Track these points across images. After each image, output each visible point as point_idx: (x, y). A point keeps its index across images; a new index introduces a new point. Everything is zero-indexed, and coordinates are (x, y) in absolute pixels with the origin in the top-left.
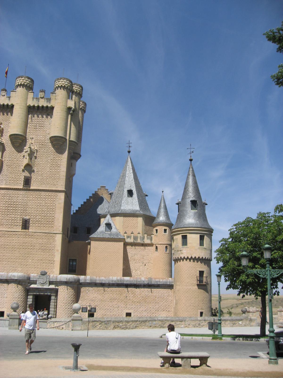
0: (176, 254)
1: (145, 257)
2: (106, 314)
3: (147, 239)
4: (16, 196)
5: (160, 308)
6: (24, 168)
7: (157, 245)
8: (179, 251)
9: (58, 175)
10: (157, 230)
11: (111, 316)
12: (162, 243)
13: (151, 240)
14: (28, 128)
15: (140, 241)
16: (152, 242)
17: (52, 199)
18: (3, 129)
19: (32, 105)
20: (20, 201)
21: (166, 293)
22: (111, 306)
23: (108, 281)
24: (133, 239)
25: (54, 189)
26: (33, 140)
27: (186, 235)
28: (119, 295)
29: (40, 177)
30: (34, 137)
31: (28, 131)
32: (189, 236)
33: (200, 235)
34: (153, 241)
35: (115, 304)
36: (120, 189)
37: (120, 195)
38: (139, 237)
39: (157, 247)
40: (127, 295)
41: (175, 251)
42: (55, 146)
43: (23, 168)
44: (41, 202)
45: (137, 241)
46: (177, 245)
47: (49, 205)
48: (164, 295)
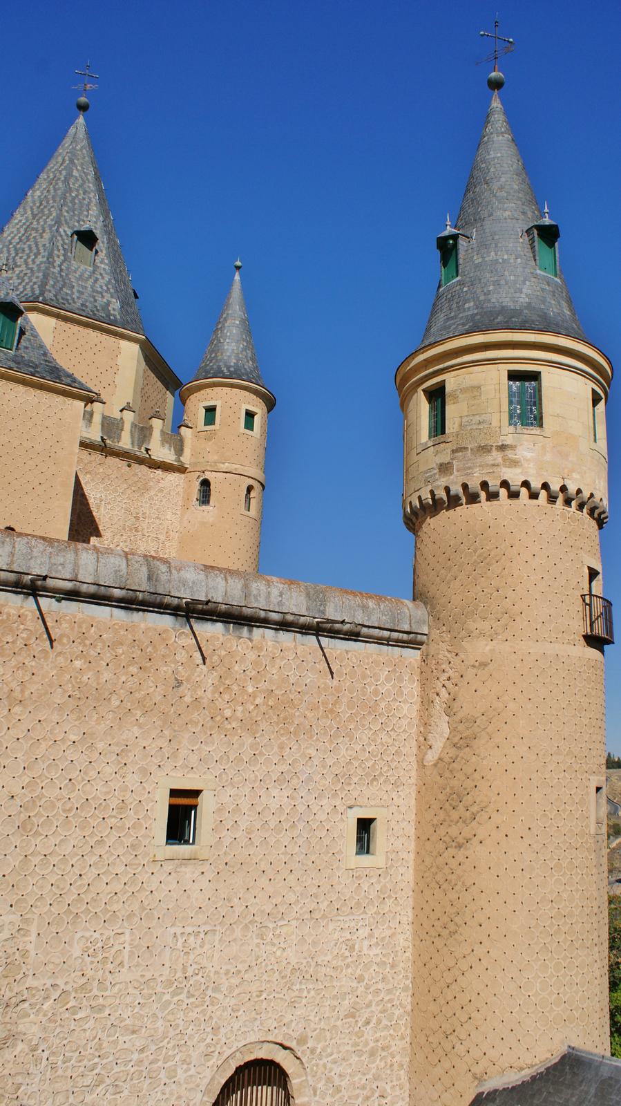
0: (469, 468)
1: (145, 525)
2: (39, 797)
3: (163, 445)
5: (356, 764)
7: (208, 475)
8: (489, 451)
10: (211, 411)
11: (70, 810)
12: (236, 469)
13: (179, 451)
15: (133, 443)
16: (182, 459)
21: (388, 679)
22: (73, 738)
23: (69, 567)
24: (100, 427)
27: (535, 376)
28: (133, 669)
32: (552, 380)
34: (186, 458)
35: (103, 727)
36: (38, 223)
37: (37, 245)
38: (127, 427)
39: (206, 483)
40: (183, 673)
41: (453, 451)
45: (118, 442)
46: (477, 418)
48: (376, 692)
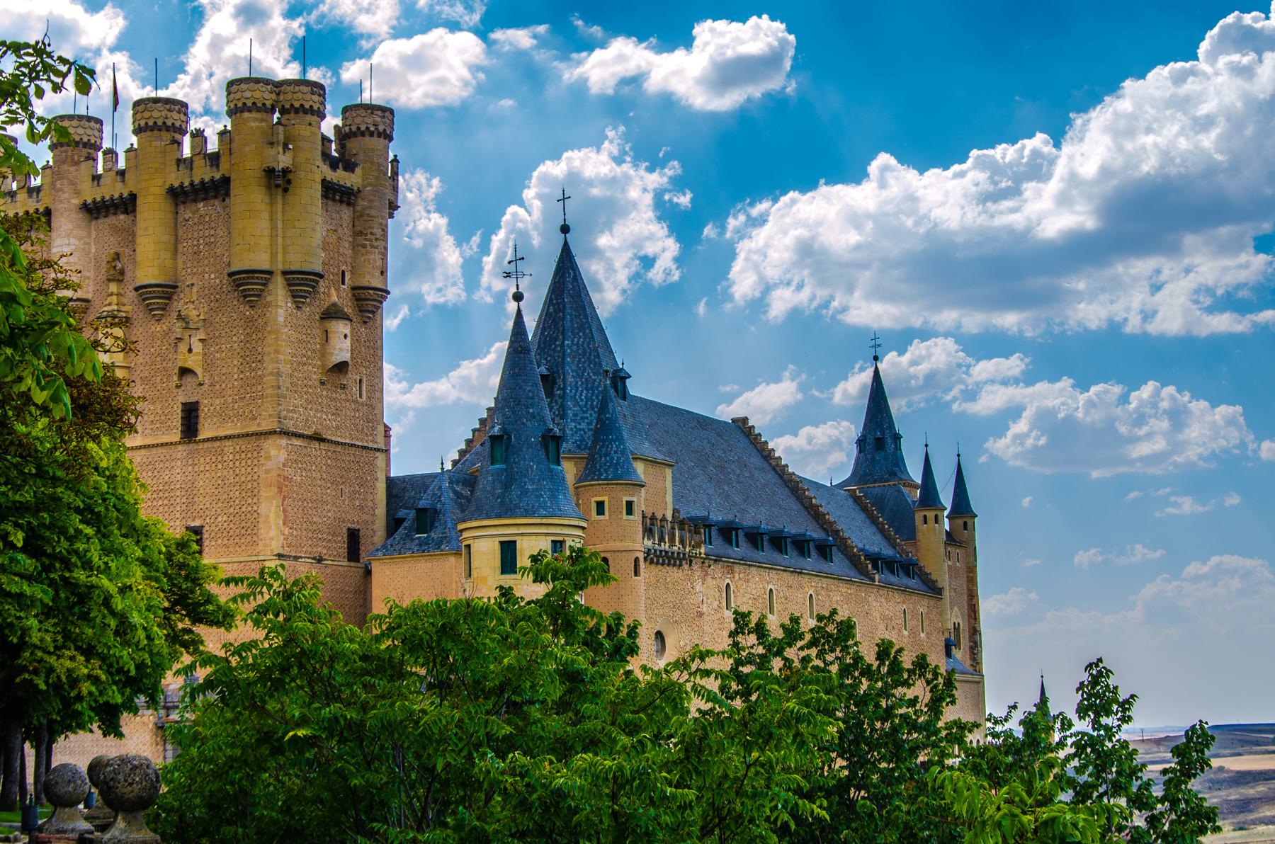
4: (167, 464)
6: (180, 378)
9: (260, 388)
14: (179, 255)
17: (249, 462)
18: (122, 273)
19: (176, 185)
20: (178, 477)
25: (254, 428)
26: (195, 289)
29: (218, 401)
30: (194, 281)
31: (180, 265)
33: (501, 543)
42: (245, 297)
43: (175, 378)
44: (225, 473)
47: (243, 479)
